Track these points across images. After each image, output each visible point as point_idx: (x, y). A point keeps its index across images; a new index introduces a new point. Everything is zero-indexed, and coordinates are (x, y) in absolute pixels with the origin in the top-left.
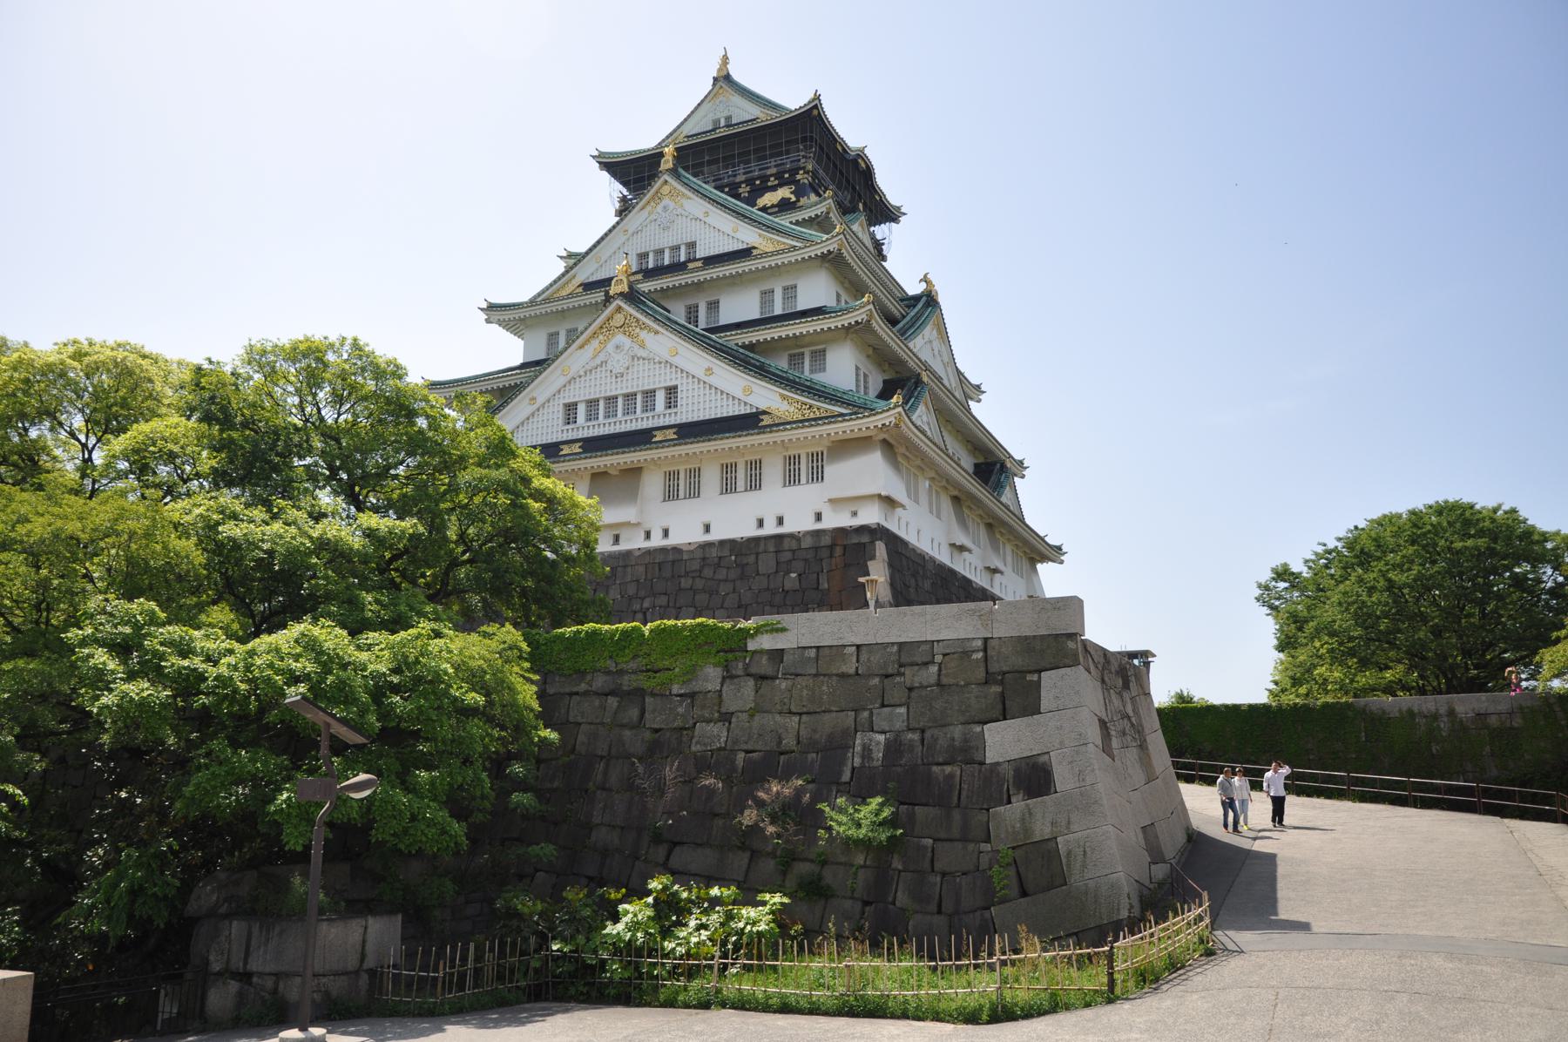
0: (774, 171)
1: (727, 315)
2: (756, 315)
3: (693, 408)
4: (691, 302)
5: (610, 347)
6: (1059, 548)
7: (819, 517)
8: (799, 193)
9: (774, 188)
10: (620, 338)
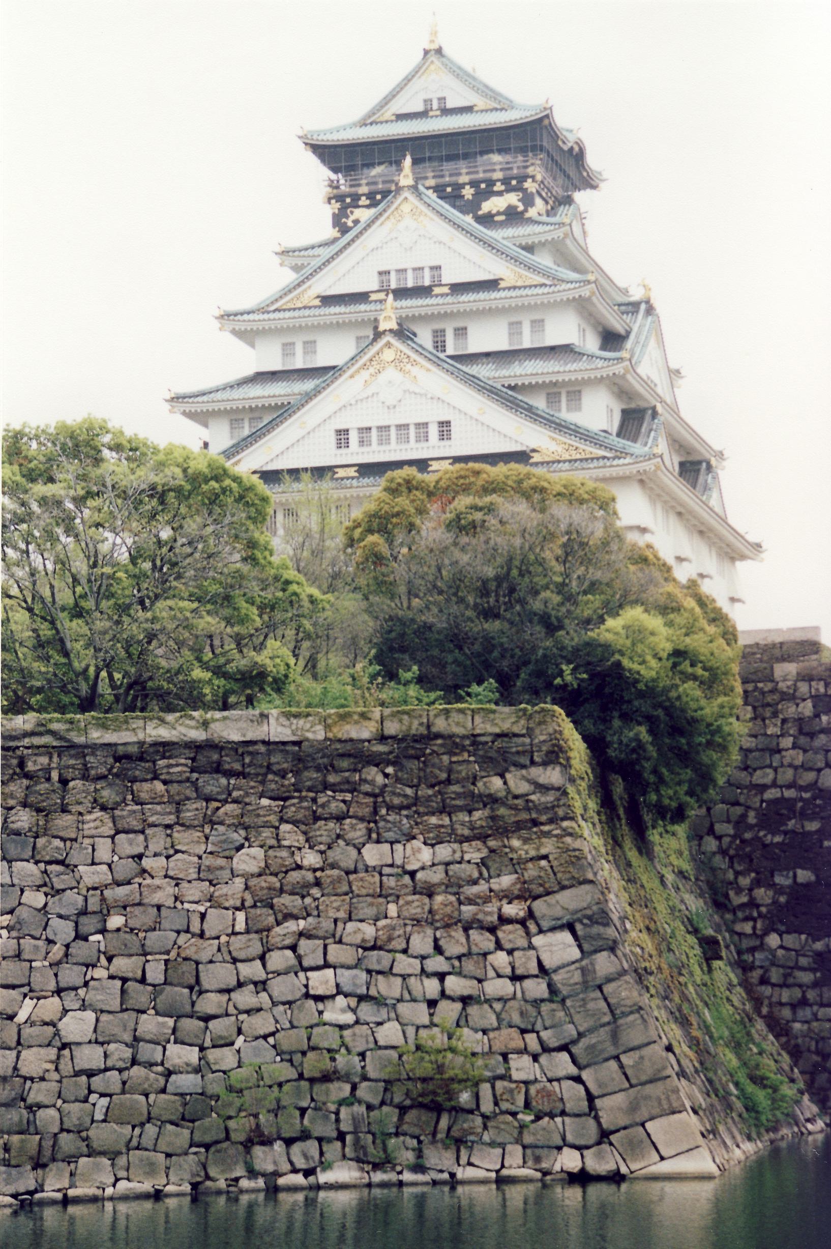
1: (475, 345)
2: (504, 346)
3: (466, 442)
4: (438, 326)
5: (382, 378)
6: (759, 546)
9: (500, 194)
10: (391, 373)
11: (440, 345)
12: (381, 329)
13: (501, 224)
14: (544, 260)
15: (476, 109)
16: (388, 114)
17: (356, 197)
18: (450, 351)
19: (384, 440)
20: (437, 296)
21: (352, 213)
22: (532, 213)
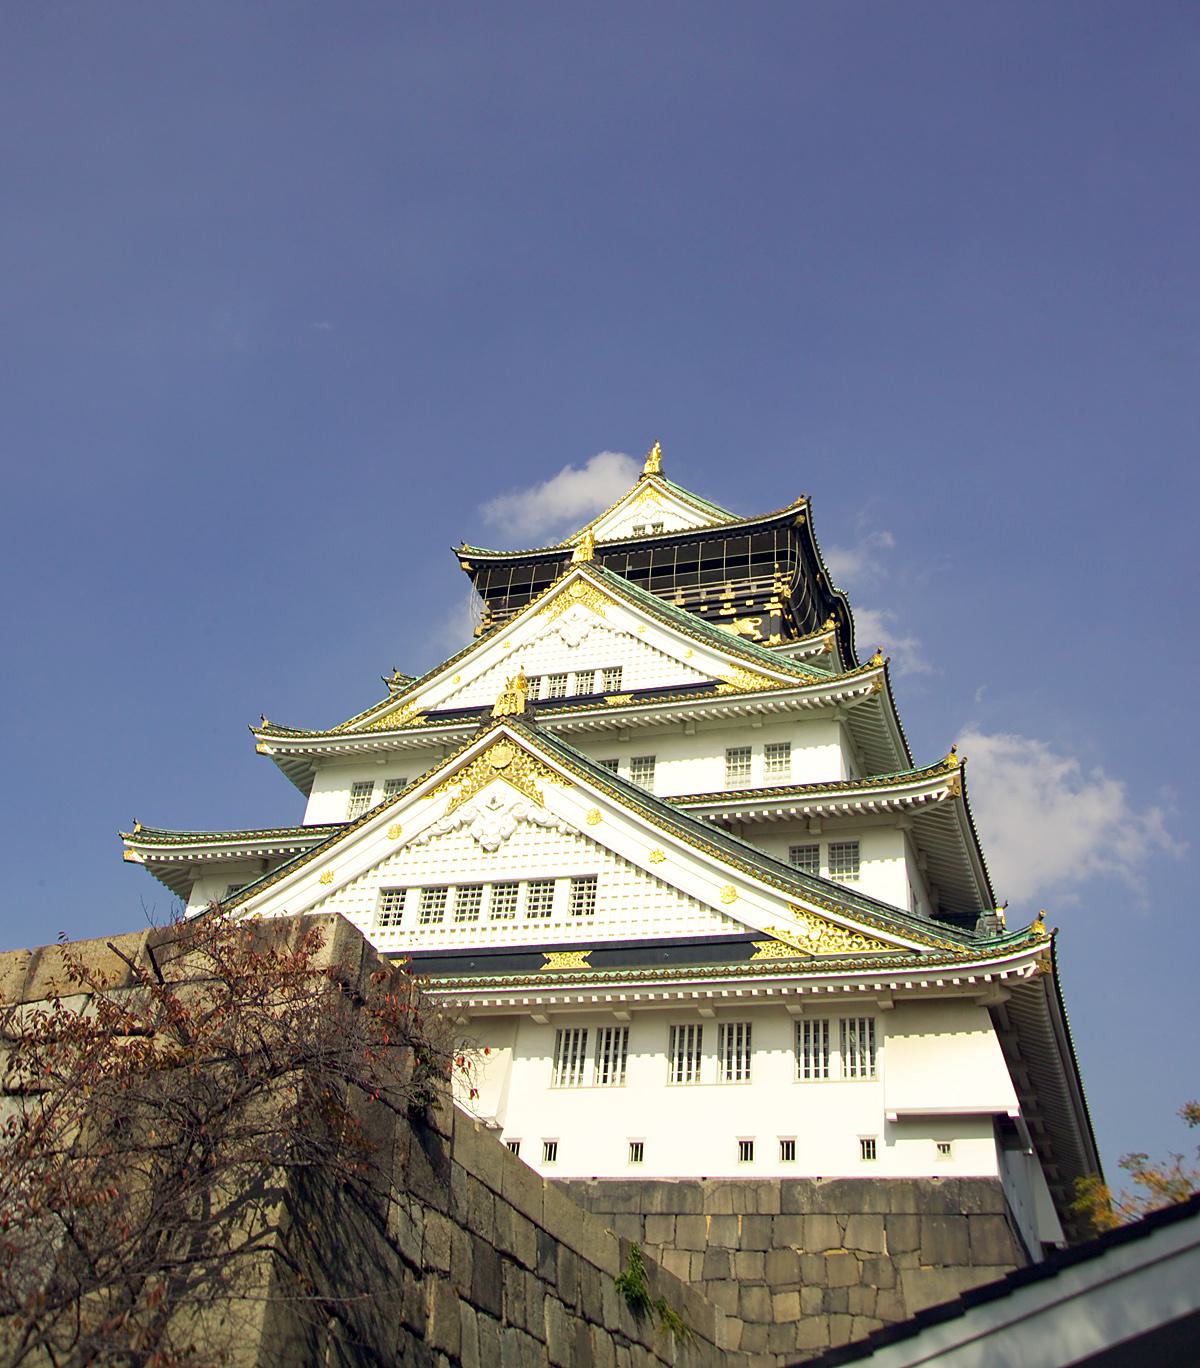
0: (732, 595)
4: (609, 755)
5: (483, 797)
7: (869, 1148)
8: (766, 631)
9: (728, 619)
10: (499, 788)
19: (468, 912)
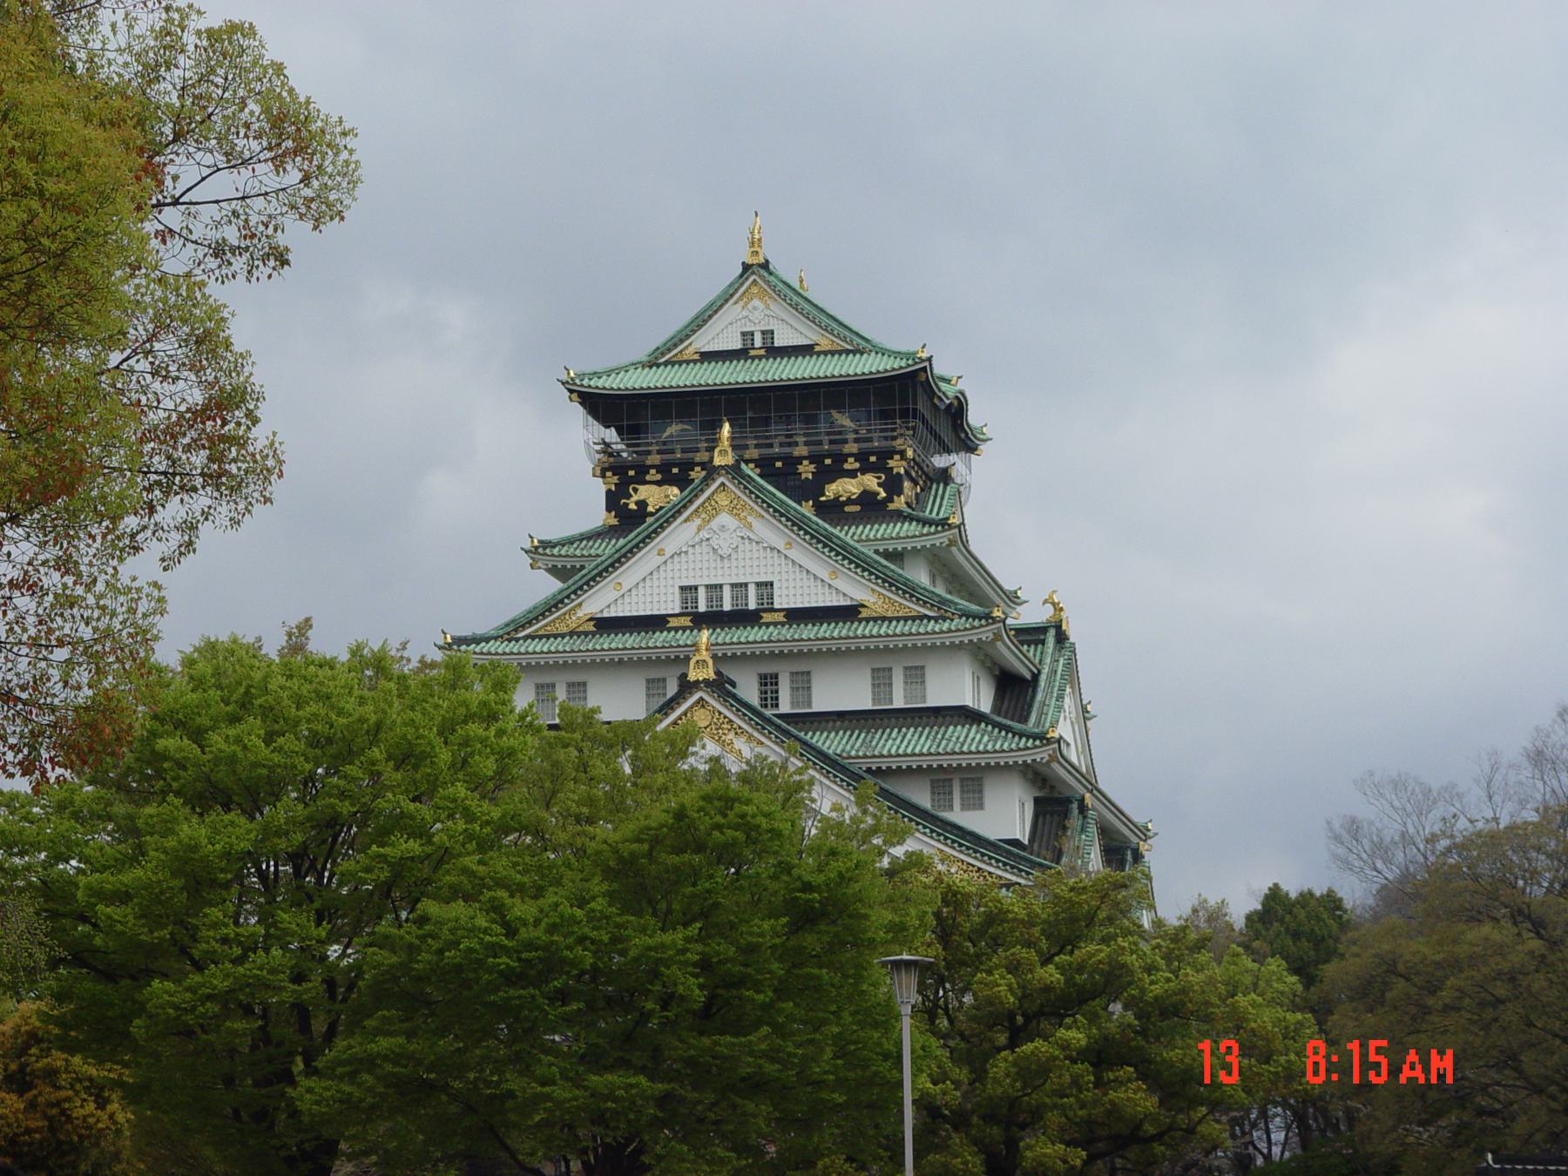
2: (866, 704)
4: (768, 669)
9: (852, 474)
11: (769, 698)
12: (692, 677)
13: (854, 519)
14: (920, 575)
15: (817, 349)
16: (689, 354)
17: (642, 470)
18: (785, 707)
20: (768, 625)
21: (636, 490)
22: (899, 503)
